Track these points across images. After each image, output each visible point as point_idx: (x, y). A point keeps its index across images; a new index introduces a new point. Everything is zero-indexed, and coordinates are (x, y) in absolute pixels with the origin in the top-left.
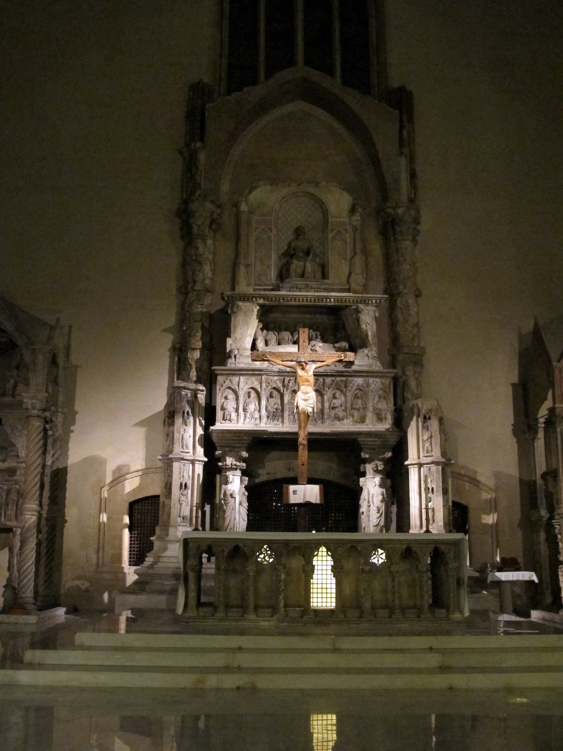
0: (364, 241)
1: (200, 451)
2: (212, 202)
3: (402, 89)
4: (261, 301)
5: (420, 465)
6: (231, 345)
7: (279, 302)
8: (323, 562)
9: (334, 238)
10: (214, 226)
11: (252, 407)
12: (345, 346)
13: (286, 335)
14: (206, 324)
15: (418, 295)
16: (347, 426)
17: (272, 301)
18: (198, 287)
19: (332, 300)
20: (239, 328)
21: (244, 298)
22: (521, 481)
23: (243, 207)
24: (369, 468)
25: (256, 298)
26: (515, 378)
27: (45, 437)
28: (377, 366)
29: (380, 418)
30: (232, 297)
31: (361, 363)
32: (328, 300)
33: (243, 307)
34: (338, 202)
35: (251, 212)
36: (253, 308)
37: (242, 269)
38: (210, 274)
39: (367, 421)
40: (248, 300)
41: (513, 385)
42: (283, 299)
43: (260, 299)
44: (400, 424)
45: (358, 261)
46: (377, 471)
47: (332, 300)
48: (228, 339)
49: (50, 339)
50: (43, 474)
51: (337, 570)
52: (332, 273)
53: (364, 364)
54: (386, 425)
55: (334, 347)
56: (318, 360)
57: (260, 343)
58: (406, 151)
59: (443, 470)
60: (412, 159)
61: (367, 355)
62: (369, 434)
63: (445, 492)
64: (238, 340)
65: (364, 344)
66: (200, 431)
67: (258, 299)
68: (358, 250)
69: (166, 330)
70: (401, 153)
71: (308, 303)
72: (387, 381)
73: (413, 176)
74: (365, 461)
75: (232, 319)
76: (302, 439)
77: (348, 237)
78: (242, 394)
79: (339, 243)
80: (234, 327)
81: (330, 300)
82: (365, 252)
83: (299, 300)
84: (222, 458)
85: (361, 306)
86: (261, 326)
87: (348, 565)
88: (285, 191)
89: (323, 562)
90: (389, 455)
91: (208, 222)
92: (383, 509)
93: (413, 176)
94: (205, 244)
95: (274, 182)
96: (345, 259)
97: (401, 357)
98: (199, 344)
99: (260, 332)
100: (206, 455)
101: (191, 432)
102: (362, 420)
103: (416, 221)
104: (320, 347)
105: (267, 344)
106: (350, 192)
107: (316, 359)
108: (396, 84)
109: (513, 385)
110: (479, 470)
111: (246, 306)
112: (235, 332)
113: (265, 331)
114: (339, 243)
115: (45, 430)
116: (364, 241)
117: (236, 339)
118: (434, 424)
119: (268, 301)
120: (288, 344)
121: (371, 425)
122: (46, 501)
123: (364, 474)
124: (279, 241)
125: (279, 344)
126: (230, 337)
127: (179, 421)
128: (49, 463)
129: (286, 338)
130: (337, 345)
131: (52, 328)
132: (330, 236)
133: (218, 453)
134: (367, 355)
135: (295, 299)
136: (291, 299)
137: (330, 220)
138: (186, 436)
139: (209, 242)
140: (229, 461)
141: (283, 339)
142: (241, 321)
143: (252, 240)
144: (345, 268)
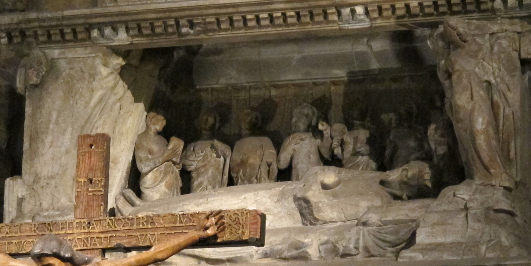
4: (122, 38)
6: (20, 201)
7: (180, 35)
12: (420, 176)
13: (256, 150)
17: (154, 34)
19: (360, 10)
20: (48, 139)
21: (62, 34)
25: (100, 27)
30: (23, 33)
31: (440, 240)
32: (346, 11)
33: (62, 64)
36: (94, 67)
40: (75, 39)
42: (192, 25)
43: (115, 30)
47: (360, 10)
48: (8, 182)
53: (449, 239)
55: (383, 183)
56: (134, 243)
57: (156, 182)
61: (466, 209)
64: (43, 183)
65: (452, 169)
67: (108, 31)
71: (280, 30)
75: (28, 110)
80: (32, 140)
81: (353, 12)
83: (245, 20)
85: (458, 23)
86: (159, 123)
99: (154, 144)
104: (325, 187)
105: (186, 184)
107: (125, 243)
111: (71, 61)
112: (34, 154)
113: (177, 143)
117: (37, 179)
119: (140, 34)
120: (259, 181)
125: (186, 188)
126: (16, 171)
129: (254, 160)
130: (394, 175)
134: (466, 209)
135: (231, 22)
136: (218, 22)
141: (243, 163)
142: (54, 115)
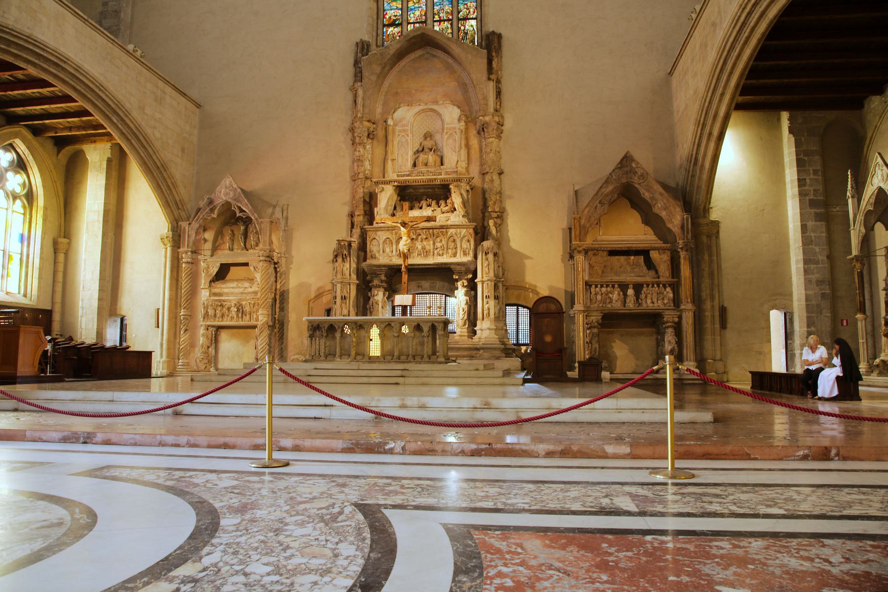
0: (467, 139)
1: (354, 276)
2: (369, 121)
3: (493, 33)
5: (483, 282)
8: (375, 332)
9: (448, 138)
10: (371, 136)
11: (388, 250)
14: (368, 200)
15: (500, 174)
16: (445, 259)
18: (361, 176)
22: (566, 291)
23: (390, 122)
24: (459, 284)
26: (565, 225)
27: (276, 272)
28: (465, 221)
29: (465, 254)
34: (451, 114)
35: (395, 125)
37: (390, 162)
38: (369, 167)
39: (458, 255)
41: (563, 229)
44: (475, 257)
45: (464, 152)
46: (463, 286)
49: (273, 213)
50: (275, 294)
51: (382, 336)
52: (446, 161)
54: (469, 258)
58: (492, 77)
59: (495, 285)
60: (498, 81)
62: (458, 264)
63: (496, 298)
66: (354, 265)
68: (463, 145)
69: (344, 204)
70: (489, 79)
72: (471, 231)
73: (499, 93)
74: (457, 281)
76: (403, 269)
77: (457, 137)
78: (381, 242)
79: (451, 141)
82: (468, 146)
84: (371, 281)
87: (389, 334)
88: (417, 109)
89: (375, 332)
90: (470, 276)
91: (366, 134)
92: (466, 309)
93: (499, 93)
94: (365, 148)
95: (410, 104)
96: (455, 152)
97: (487, 214)
98: (362, 212)
100: (358, 279)
101: (348, 266)
102: (455, 255)
103: (500, 124)
106: (459, 107)
108: (491, 30)
109: (563, 229)
110: (538, 285)
114: (451, 141)
115: (275, 268)
116: (467, 139)
118: (491, 256)
121: (460, 258)
122: (277, 310)
123: (457, 289)
124: (413, 142)
127: (340, 259)
128: (278, 287)
131: (275, 207)
132: (446, 137)
133: (368, 278)
137: (446, 126)
138: (345, 269)
139: (368, 147)
140: (376, 282)
143: (395, 143)
144: (455, 158)
